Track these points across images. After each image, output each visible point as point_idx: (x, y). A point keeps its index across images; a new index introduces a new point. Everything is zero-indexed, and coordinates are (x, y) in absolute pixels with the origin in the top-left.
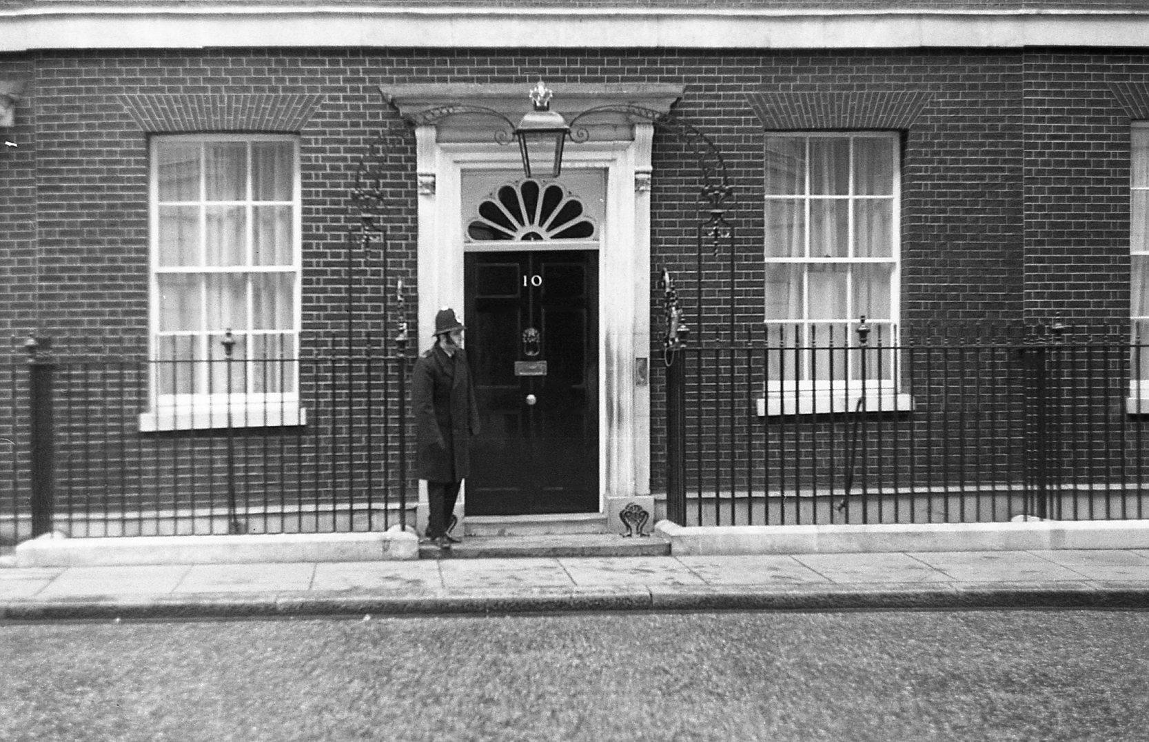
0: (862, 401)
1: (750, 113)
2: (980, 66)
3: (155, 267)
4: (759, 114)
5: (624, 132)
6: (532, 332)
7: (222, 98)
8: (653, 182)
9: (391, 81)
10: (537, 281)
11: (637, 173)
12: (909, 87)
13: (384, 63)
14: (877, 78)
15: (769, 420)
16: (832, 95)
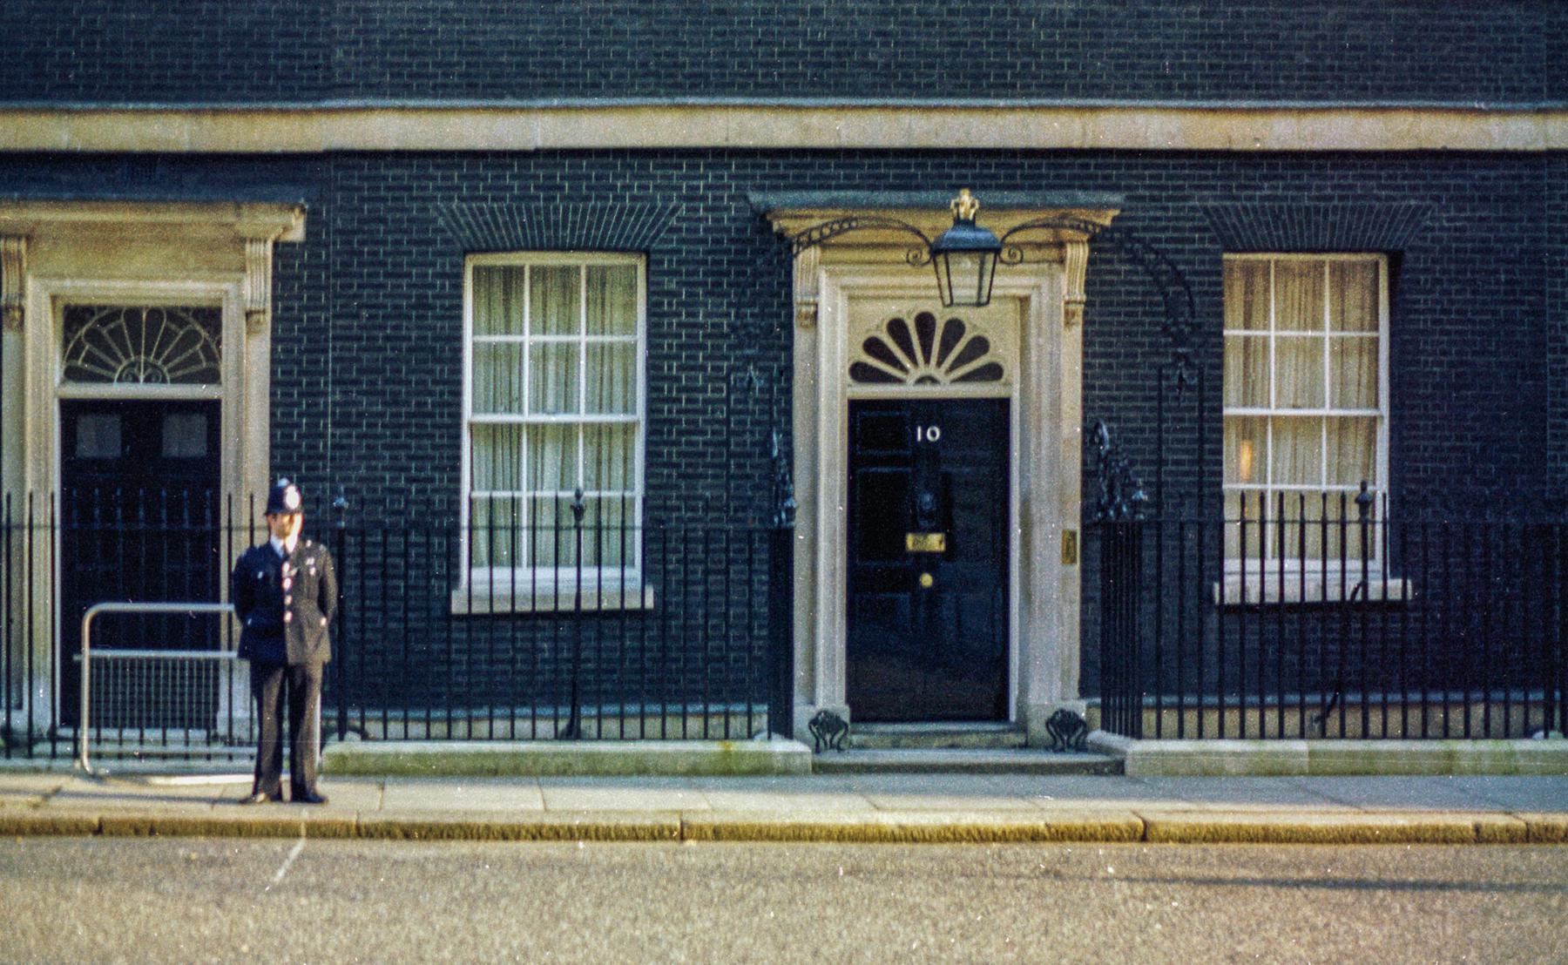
0: (1364, 584)
1: (1206, 229)
2: (1493, 173)
3: (468, 414)
4: (1217, 229)
5: (1054, 253)
6: (928, 498)
7: (556, 209)
8: (1085, 313)
9: (761, 188)
10: (933, 434)
11: (1067, 303)
12: (1404, 198)
13: (754, 166)
14: (1363, 187)
15: (1225, 610)
16: (1308, 209)
